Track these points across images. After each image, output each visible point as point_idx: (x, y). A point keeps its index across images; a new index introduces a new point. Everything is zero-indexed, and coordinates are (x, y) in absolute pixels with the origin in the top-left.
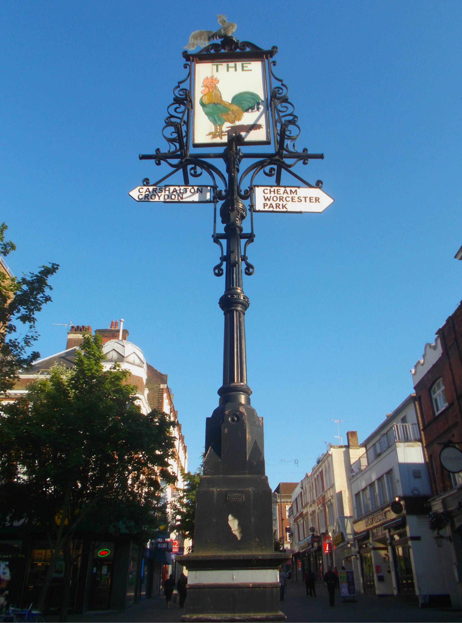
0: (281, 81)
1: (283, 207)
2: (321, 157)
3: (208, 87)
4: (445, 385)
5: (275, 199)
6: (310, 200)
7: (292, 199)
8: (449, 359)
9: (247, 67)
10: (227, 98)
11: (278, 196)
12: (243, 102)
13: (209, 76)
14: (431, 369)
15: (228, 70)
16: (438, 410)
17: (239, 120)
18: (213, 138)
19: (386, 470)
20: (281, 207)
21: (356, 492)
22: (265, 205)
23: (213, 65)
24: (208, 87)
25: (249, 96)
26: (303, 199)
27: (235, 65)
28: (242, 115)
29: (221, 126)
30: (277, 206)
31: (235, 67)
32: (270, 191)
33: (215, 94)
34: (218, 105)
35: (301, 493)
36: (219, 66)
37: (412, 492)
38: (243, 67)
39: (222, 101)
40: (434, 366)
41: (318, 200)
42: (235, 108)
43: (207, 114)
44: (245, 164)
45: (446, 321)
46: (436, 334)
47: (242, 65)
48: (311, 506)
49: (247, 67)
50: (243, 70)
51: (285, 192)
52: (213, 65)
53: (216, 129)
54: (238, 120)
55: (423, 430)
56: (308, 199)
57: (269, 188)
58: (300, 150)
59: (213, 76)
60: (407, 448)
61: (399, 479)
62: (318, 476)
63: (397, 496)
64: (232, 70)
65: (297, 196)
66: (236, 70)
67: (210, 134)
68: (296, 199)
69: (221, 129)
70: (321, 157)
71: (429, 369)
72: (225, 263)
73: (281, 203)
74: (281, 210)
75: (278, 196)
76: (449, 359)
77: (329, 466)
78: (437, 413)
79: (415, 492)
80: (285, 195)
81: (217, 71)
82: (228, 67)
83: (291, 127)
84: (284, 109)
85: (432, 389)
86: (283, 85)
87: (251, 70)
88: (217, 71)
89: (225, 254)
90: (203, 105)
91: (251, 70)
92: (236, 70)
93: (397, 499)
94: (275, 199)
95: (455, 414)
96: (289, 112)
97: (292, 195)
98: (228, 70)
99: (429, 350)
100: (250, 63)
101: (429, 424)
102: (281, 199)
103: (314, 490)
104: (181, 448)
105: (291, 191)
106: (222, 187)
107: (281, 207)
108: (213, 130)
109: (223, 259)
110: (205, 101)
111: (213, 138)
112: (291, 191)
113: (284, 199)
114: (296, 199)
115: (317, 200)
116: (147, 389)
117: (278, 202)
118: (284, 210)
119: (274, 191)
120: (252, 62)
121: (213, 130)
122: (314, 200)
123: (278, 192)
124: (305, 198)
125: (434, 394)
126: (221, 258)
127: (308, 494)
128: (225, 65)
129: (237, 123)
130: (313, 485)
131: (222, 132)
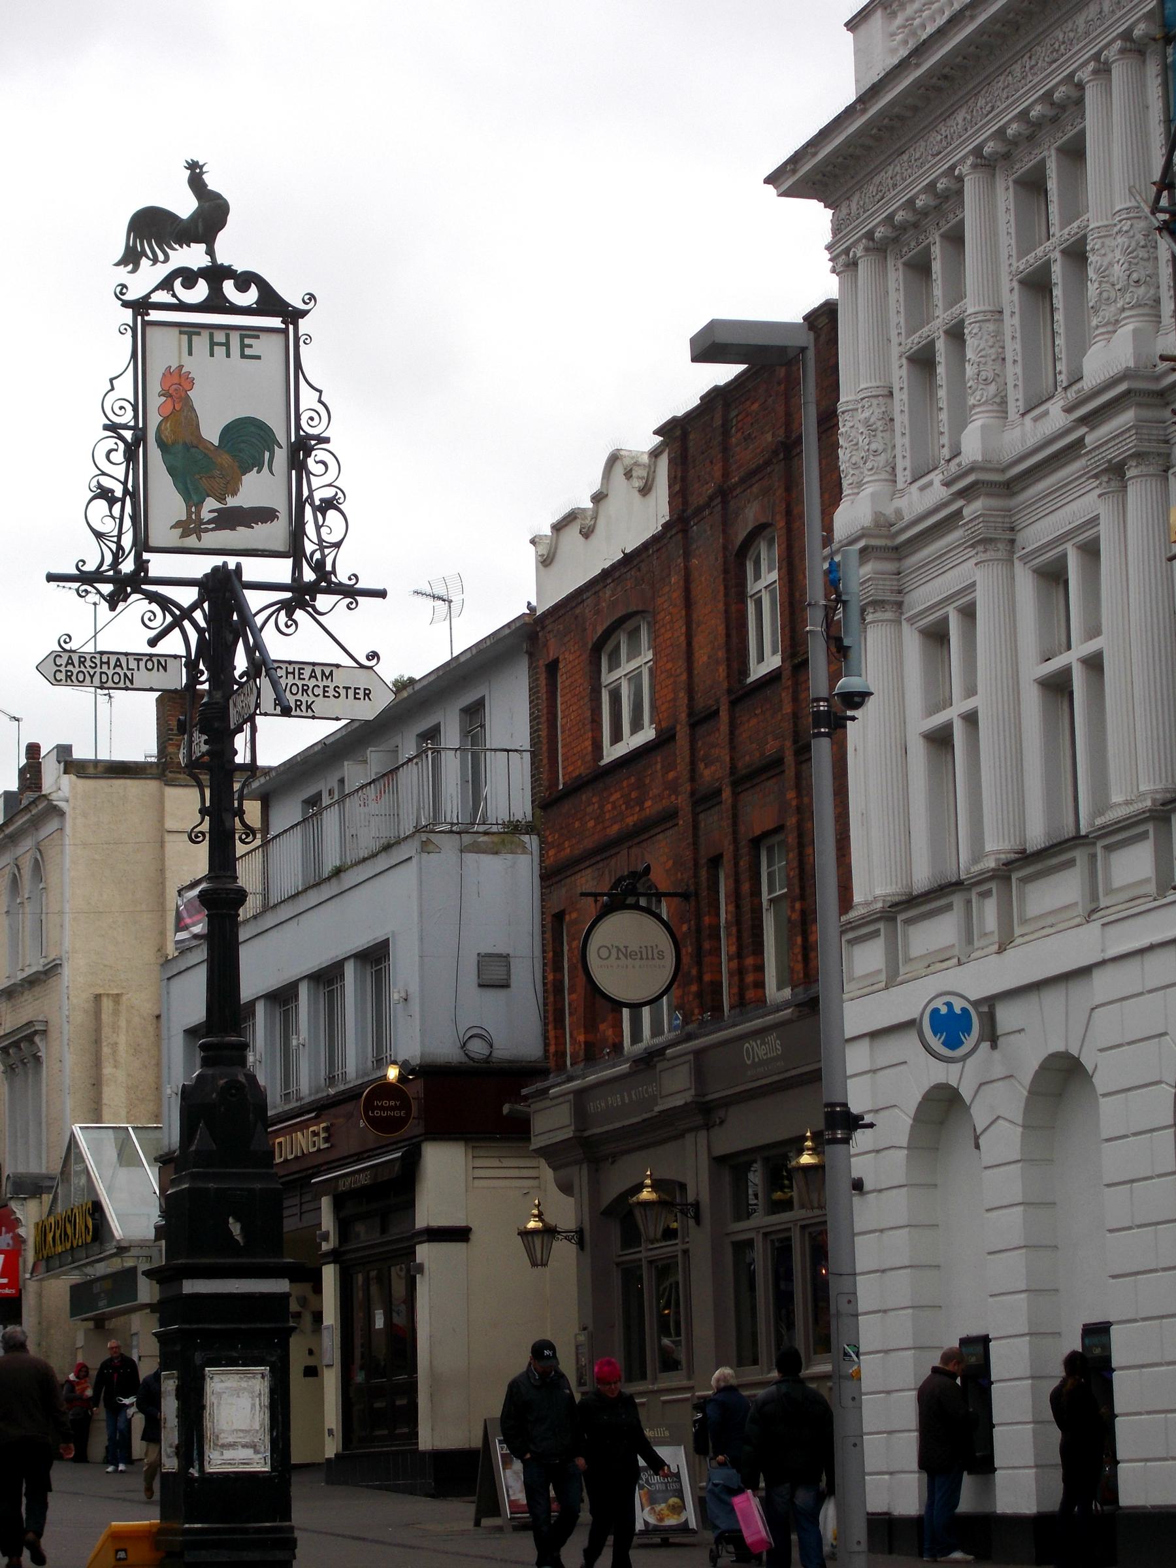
0: (320, 392)
1: (309, 707)
2: (382, 594)
3: (171, 396)
4: (655, 647)
5: (294, 690)
6: (355, 693)
7: (325, 691)
8: (687, 556)
9: (250, 346)
10: (211, 433)
11: (300, 683)
12: (242, 445)
14: (614, 567)
15: (212, 355)
16: (617, 737)
17: (234, 493)
18: (183, 536)
19: (362, 940)
20: (304, 707)
23: (181, 333)
24: (171, 396)
25: (253, 429)
26: (343, 692)
27: (227, 336)
28: (241, 480)
29: (199, 505)
31: (227, 344)
32: (287, 673)
33: (186, 418)
34: (193, 450)
36: (194, 338)
38: (243, 346)
39: (199, 436)
40: (628, 559)
41: (368, 695)
42: (225, 459)
43: (171, 471)
45: (702, 398)
46: (656, 432)
47: (242, 338)
49: (250, 346)
50: (243, 356)
51: (313, 676)
52: (181, 333)
53: (189, 513)
54: (233, 495)
56: (351, 693)
57: (284, 666)
60: (470, 857)
61: (414, 989)
63: (394, 1063)
64: (220, 351)
65: (332, 686)
66: (228, 356)
67: (178, 524)
68: (331, 693)
69: (198, 513)
70: (382, 594)
71: (607, 565)
72: (207, 818)
73: (304, 699)
74: (304, 714)
75: (300, 683)
76: (687, 556)
78: (612, 753)
79: (478, 1048)
80: (313, 682)
81: (190, 353)
82: (213, 344)
83: (331, 513)
84: (321, 468)
85: (609, 647)
86: (320, 401)
87: (259, 357)
88: (190, 353)
89: (208, 804)
90: (161, 444)
91: (259, 357)
92: (228, 356)
93: (393, 1073)
94: (294, 690)
95: (671, 775)
97: (325, 683)
98: (212, 355)
99: (623, 491)
100: (258, 337)
101: (577, 787)
102: (305, 691)
105: (323, 673)
107: (304, 707)
108: (184, 518)
109: (203, 811)
111: (183, 536)
112: (323, 673)
113: (310, 692)
114: (331, 693)
115: (367, 694)
117: (299, 697)
118: (310, 713)
119: (293, 673)
120: (263, 336)
121: (184, 518)
122: (361, 696)
123: (300, 674)
124: (347, 688)
125: (610, 670)
126: (200, 811)
128: (205, 334)
129: (232, 502)
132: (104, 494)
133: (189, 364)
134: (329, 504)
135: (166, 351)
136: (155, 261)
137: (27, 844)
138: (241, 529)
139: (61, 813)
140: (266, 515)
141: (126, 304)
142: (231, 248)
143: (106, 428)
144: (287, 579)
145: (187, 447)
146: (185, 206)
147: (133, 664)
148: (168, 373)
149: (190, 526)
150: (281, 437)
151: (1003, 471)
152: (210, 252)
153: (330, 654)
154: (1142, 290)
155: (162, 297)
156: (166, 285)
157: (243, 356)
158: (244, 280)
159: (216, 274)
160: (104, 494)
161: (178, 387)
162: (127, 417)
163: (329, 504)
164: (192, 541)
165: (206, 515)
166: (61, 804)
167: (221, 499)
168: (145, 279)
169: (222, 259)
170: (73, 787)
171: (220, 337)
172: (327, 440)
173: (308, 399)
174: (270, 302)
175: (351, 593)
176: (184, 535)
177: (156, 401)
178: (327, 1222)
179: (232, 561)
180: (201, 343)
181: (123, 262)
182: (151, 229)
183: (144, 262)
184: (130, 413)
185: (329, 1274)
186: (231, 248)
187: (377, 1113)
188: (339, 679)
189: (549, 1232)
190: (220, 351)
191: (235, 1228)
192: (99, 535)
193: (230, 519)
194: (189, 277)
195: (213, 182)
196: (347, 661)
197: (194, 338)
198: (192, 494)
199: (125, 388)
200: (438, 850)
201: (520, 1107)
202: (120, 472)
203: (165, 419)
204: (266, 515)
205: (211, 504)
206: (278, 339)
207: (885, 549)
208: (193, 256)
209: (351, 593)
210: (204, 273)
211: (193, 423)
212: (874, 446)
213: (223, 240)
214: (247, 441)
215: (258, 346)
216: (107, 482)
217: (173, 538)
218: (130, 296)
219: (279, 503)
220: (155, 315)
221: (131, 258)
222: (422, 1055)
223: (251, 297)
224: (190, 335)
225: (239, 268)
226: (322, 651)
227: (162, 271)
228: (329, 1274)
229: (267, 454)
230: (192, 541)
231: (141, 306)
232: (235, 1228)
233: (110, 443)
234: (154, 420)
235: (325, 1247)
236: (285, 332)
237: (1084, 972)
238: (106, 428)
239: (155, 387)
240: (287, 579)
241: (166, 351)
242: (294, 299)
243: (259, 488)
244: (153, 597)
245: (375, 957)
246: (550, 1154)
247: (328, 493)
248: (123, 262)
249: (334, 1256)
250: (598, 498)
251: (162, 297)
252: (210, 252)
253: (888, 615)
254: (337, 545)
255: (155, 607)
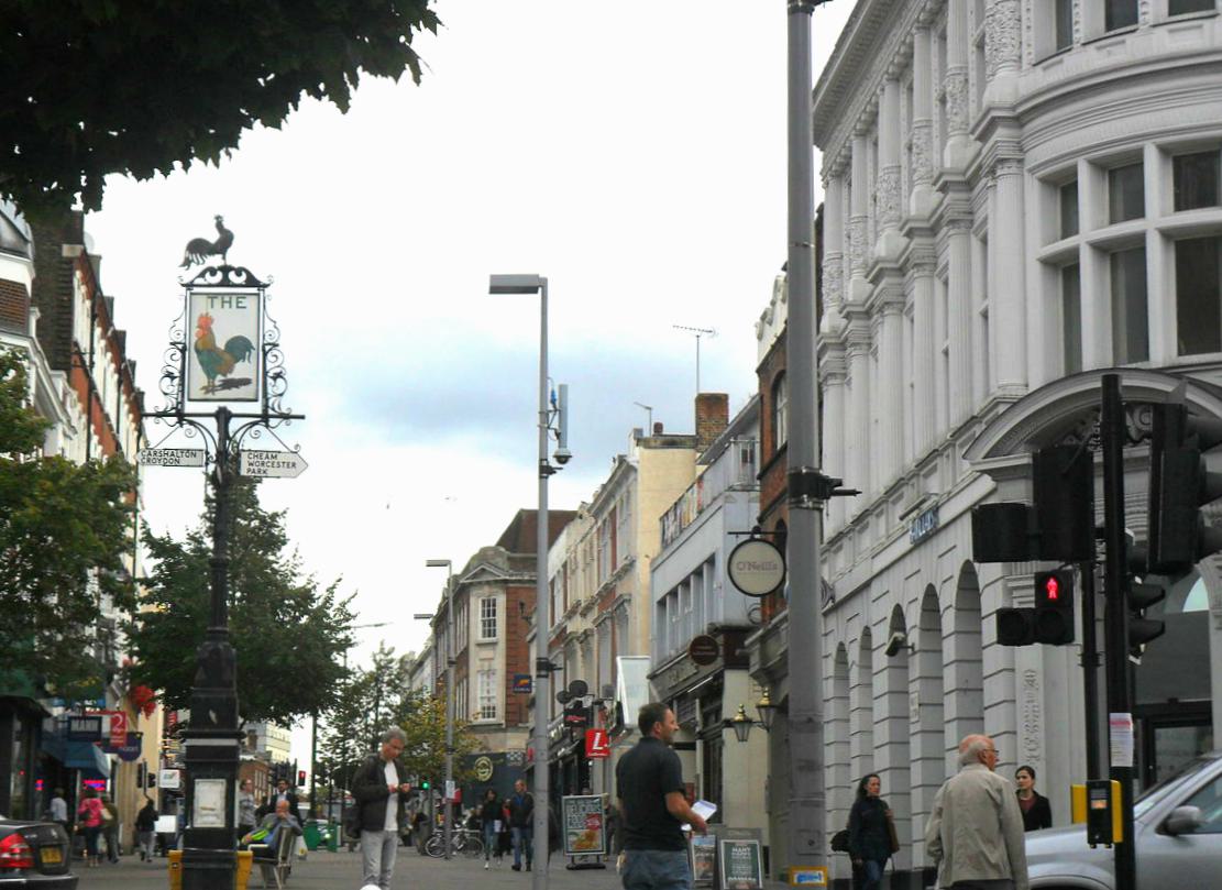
2: (302, 417)
10: (221, 344)
13: (204, 312)
15: (223, 307)
17: (231, 372)
19: (706, 555)
21: (659, 597)
22: (249, 470)
29: (214, 378)
30: (259, 472)
31: (230, 302)
35: (565, 566)
37: (749, 614)
38: (238, 302)
42: (227, 357)
43: (202, 363)
44: (234, 424)
48: (584, 615)
50: (238, 307)
51: (267, 457)
55: (760, 477)
58: (286, 412)
59: (207, 314)
62: (604, 522)
64: (227, 305)
67: (204, 388)
68: (276, 465)
70: (302, 417)
77: (628, 498)
81: (212, 306)
82: (223, 302)
83: (279, 380)
84: (274, 359)
88: (212, 306)
90: (197, 351)
96: (277, 364)
98: (223, 307)
102: (263, 464)
103: (595, 563)
104: (100, 344)
106: (213, 452)
108: (206, 384)
110: (200, 347)
115: (294, 465)
116: (37, 309)
121: (206, 384)
127: (579, 572)
128: (220, 297)
129: (229, 376)
130: (591, 548)
131: (214, 386)
132: (170, 375)
133: (212, 313)
134: (278, 376)
135: (202, 306)
136: (198, 263)
137: (624, 489)
138: (234, 390)
139: (635, 470)
140: (246, 382)
141: (183, 285)
142: (234, 257)
143: (172, 344)
144: (259, 412)
145: (210, 351)
146: (213, 237)
147: (180, 454)
148: (201, 317)
149: (210, 389)
150: (254, 344)
151: (863, 305)
152: (224, 258)
153: (276, 446)
154: (893, 212)
155: (200, 281)
156: (202, 275)
157: (238, 307)
158: (238, 272)
159: (226, 269)
160: (170, 375)
161: (206, 324)
162: (181, 339)
163: (278, 376)
164: (210, 396)
165: (217, 383)
166: (635, 464)
167: (224, 375)
168: (196, 269)
169: (230, 262)
170: (641, 454)
171: (227, 299)
172: (277, 345)
173: (269, 326)
174: (252, 281)
175: (286, 417)
176: (207, 392)
177: (195, 330)
178: (698, 716)
179: (222, 404)
180: (218, 302)
181: (184, 265)
182: (198, 247)
183: (193, 265)
184: (182, 337)
185: (699, 744)
186: (234, 257)
187: (698, 653)
188: (280, 458)
189: (747, 722)
190: (227, 305)
191: (213, 715)
192: (166, 394)
193: (228, 384)
194: (213, 271)
195: (227, 225)
196: (283, 449)
197: (215, 300)
198: (211, 374)
199: (181, 325)
200: (735, 502)
201: (747, 651)
202: (178, 365)
203: (199, 339)
204: (246, 382)
205: (220, 377)
206: (255, 298)
207: (836, 344)
208: (215, 261)
209: (286, 417)
210: (221, 269)
211: (213, 340)
212: (833, 287)
213: (230, 252)
214: (239, 348)
215: (245, 302)
216: (170, 369)
217: (201, 395)
218: (186, 281)
219: (252, 376)
220: (196, 290)
221: (187, 263)
222: (725, 619)
223: (242, 279)
224: (212, 298)
225: (236, 266)
226: (273, 446)
227: (201, 268)
228: (699, 744)
229: (247, 354)
230: (210, 396)
231: (189, 286)
232: (213, 715)
233: (172, 351)
234: (194, 339)
235: (698, 729)
236: (258, 295)
237: (867, 585)
238: (172, 344)
239: (195, 324)
240: (259, 412)
241: (202, 306)
242: (263, 279)
243: (241, 370)
244: (191, 423)
245: (711, 561)
246: (754, 676)
247: (278, 370)
248: (184, 265)
249: (701, 735)
250: (773, 303)
251: (200, 281)
252: (224, 258)
253: (838, 381)
254: (281, 395)
255: (192, 427)
